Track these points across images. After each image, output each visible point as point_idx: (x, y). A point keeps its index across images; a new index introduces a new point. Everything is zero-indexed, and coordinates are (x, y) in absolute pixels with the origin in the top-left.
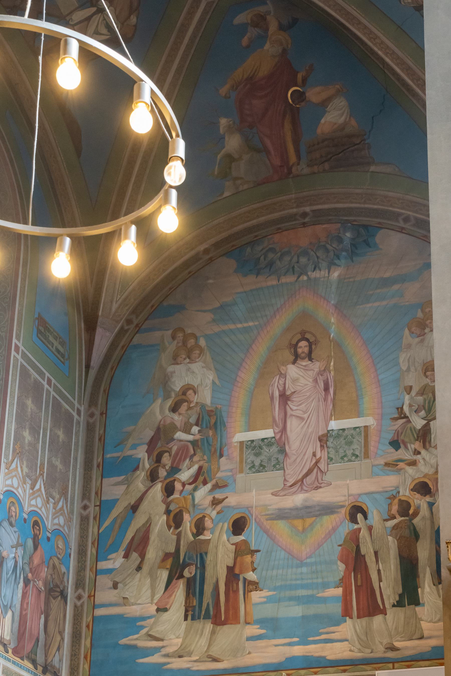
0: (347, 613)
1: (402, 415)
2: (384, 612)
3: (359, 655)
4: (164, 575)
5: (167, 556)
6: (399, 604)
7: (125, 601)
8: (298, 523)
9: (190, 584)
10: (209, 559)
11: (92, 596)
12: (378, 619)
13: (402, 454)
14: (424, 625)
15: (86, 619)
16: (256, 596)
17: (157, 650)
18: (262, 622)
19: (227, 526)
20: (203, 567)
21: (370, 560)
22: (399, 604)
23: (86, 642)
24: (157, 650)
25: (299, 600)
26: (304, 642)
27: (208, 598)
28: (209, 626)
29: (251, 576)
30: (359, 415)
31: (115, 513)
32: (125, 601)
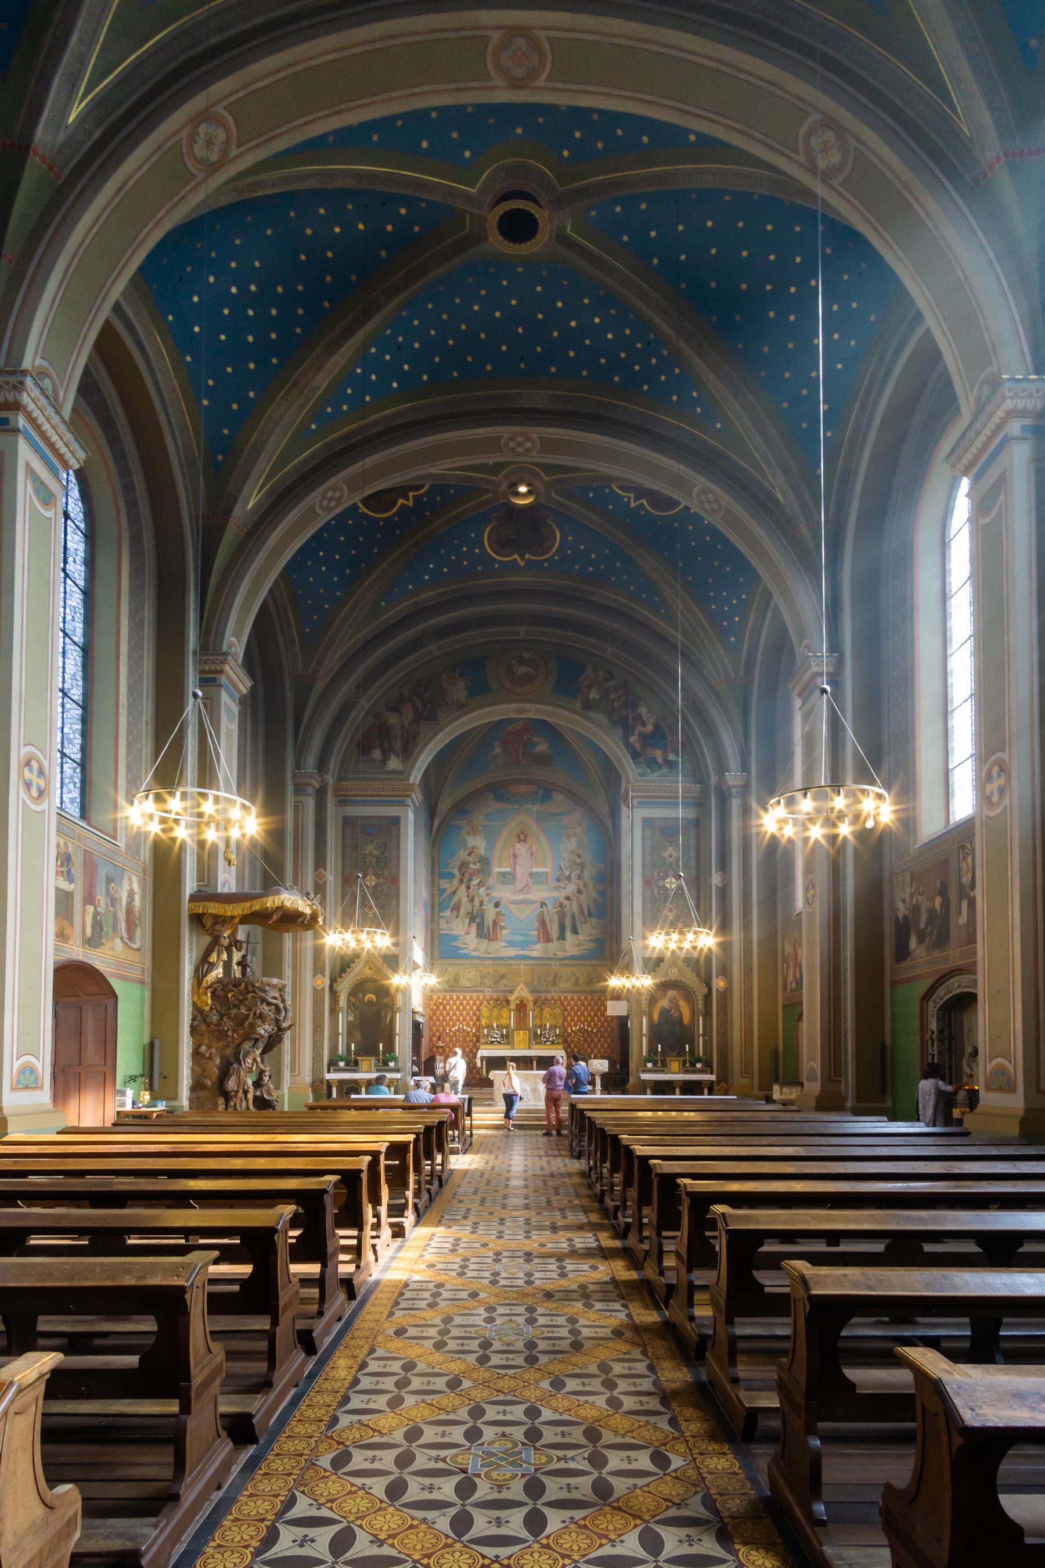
0: (539, 941)
1: (560, 869)
2: (552, 941)
3: (542, 956)
4: (468, 921)
5: (468, 913)
6: (558, 939)
7: (452, 929)
8: (521, 906)
9: (478, 925)
10: (486, 916)
11: (438, 926)
12: (550, 944)
13: (560, 884)
14: (567, 947)
15: (436, 935)
16: (504, 932)
17: (465, 948)
18: (506, 941)
19: (493, 904)
20: (483, 919)
21: (548, 923)
22: (558, 939)
23: (436, 943)
24: (465, 948)
25: (520, 934)
26: (523, 950)
27: (485, 931)
28: (486, 941)
29: (503, 924)
30: (545, 867)
31: (447, 893)
32: (452, 929)
